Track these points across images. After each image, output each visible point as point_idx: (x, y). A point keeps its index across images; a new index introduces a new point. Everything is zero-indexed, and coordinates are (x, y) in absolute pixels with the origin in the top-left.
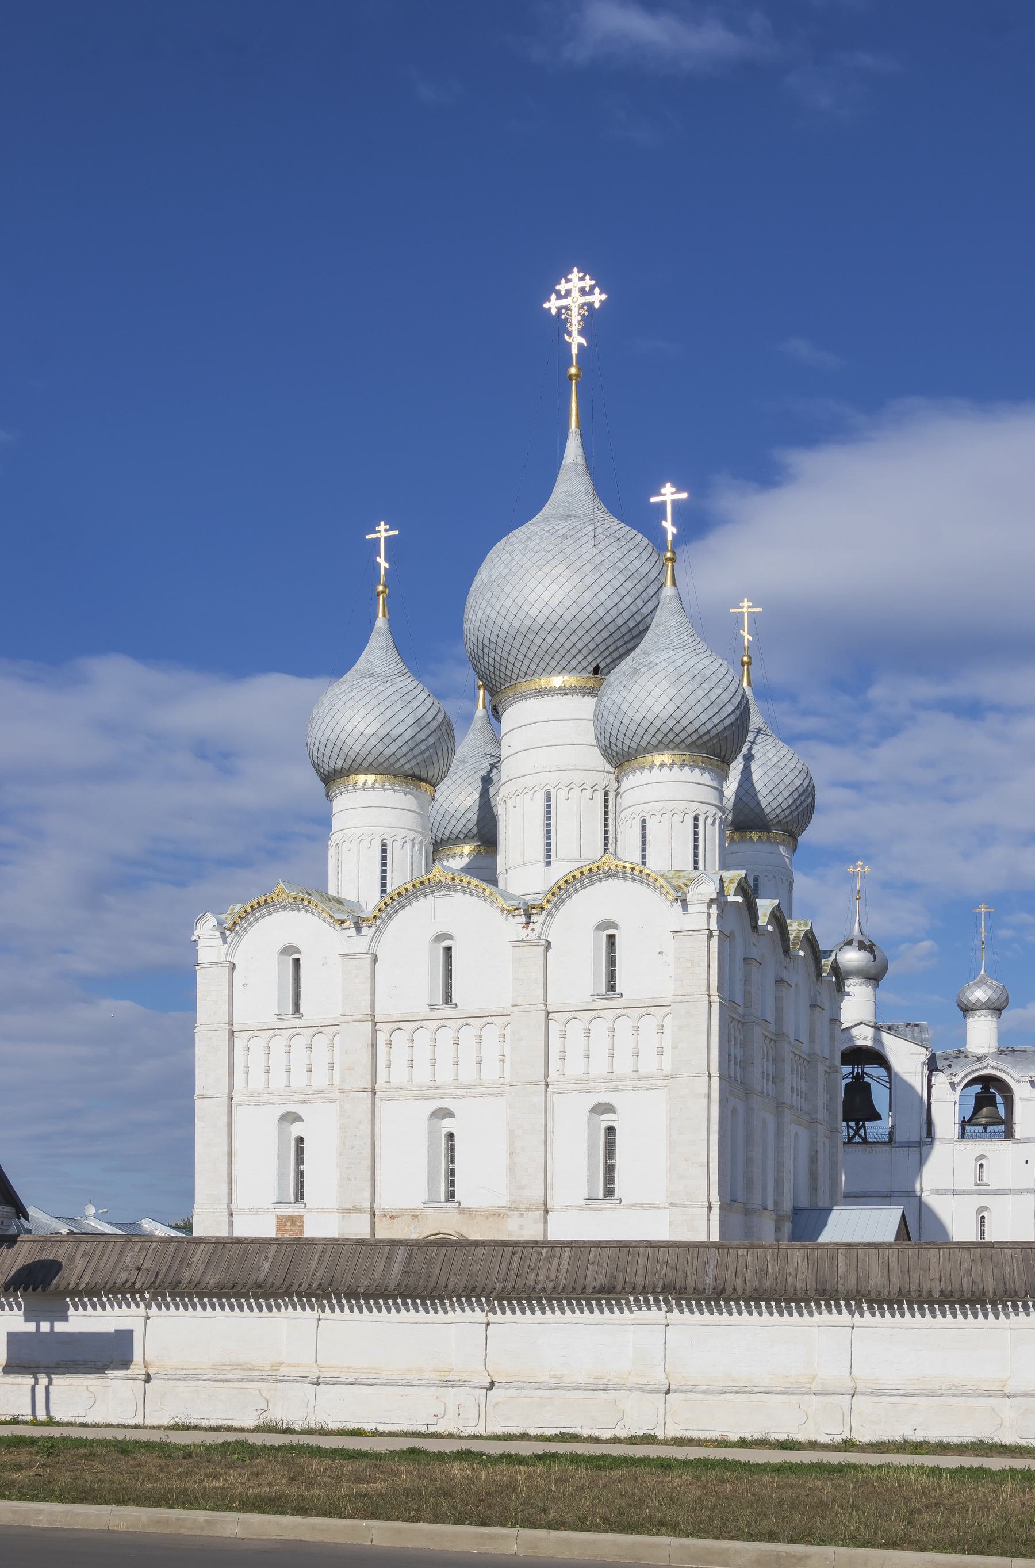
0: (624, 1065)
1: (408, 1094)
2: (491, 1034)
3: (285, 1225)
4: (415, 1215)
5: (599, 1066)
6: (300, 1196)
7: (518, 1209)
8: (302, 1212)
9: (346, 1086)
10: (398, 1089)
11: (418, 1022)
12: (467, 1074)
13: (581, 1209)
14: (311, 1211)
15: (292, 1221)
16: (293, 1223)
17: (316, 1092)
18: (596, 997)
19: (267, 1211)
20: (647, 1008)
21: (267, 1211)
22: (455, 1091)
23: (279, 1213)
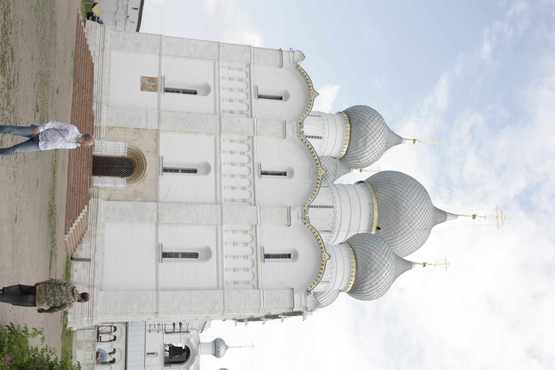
0: (228, 263)
1: (217, 151)
2: (246, 195)
3: (153, 82)
4: (156, 151)
5: (228, 250)
6: (167, 90)
7: (157, 208)
8: (159, 91)
9: (223, 119)
10: (220, 146)
11: (252, 159)
12: (226, 181)
13: (157, 240)
14: (159, 97)
15: (155, 86)
16: (154, 86)
17: (220, 104)
18: (263, 249)
19: (160, 73)
20: (256, 276)
21: (160, 73)
22: (218, 175)
23: (160, 79)
